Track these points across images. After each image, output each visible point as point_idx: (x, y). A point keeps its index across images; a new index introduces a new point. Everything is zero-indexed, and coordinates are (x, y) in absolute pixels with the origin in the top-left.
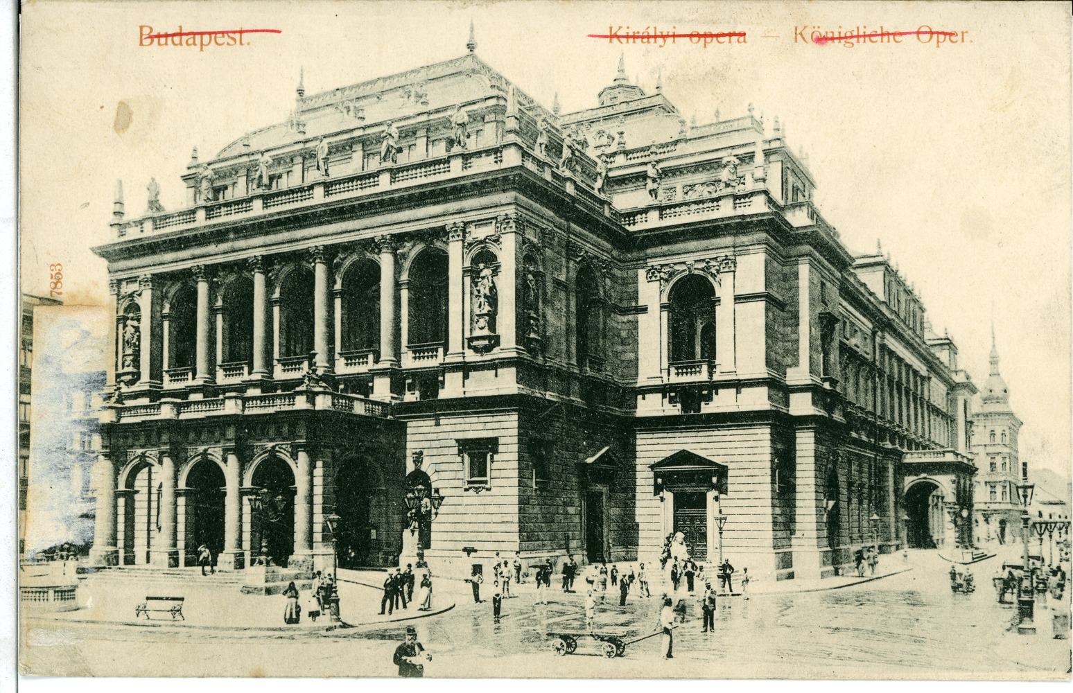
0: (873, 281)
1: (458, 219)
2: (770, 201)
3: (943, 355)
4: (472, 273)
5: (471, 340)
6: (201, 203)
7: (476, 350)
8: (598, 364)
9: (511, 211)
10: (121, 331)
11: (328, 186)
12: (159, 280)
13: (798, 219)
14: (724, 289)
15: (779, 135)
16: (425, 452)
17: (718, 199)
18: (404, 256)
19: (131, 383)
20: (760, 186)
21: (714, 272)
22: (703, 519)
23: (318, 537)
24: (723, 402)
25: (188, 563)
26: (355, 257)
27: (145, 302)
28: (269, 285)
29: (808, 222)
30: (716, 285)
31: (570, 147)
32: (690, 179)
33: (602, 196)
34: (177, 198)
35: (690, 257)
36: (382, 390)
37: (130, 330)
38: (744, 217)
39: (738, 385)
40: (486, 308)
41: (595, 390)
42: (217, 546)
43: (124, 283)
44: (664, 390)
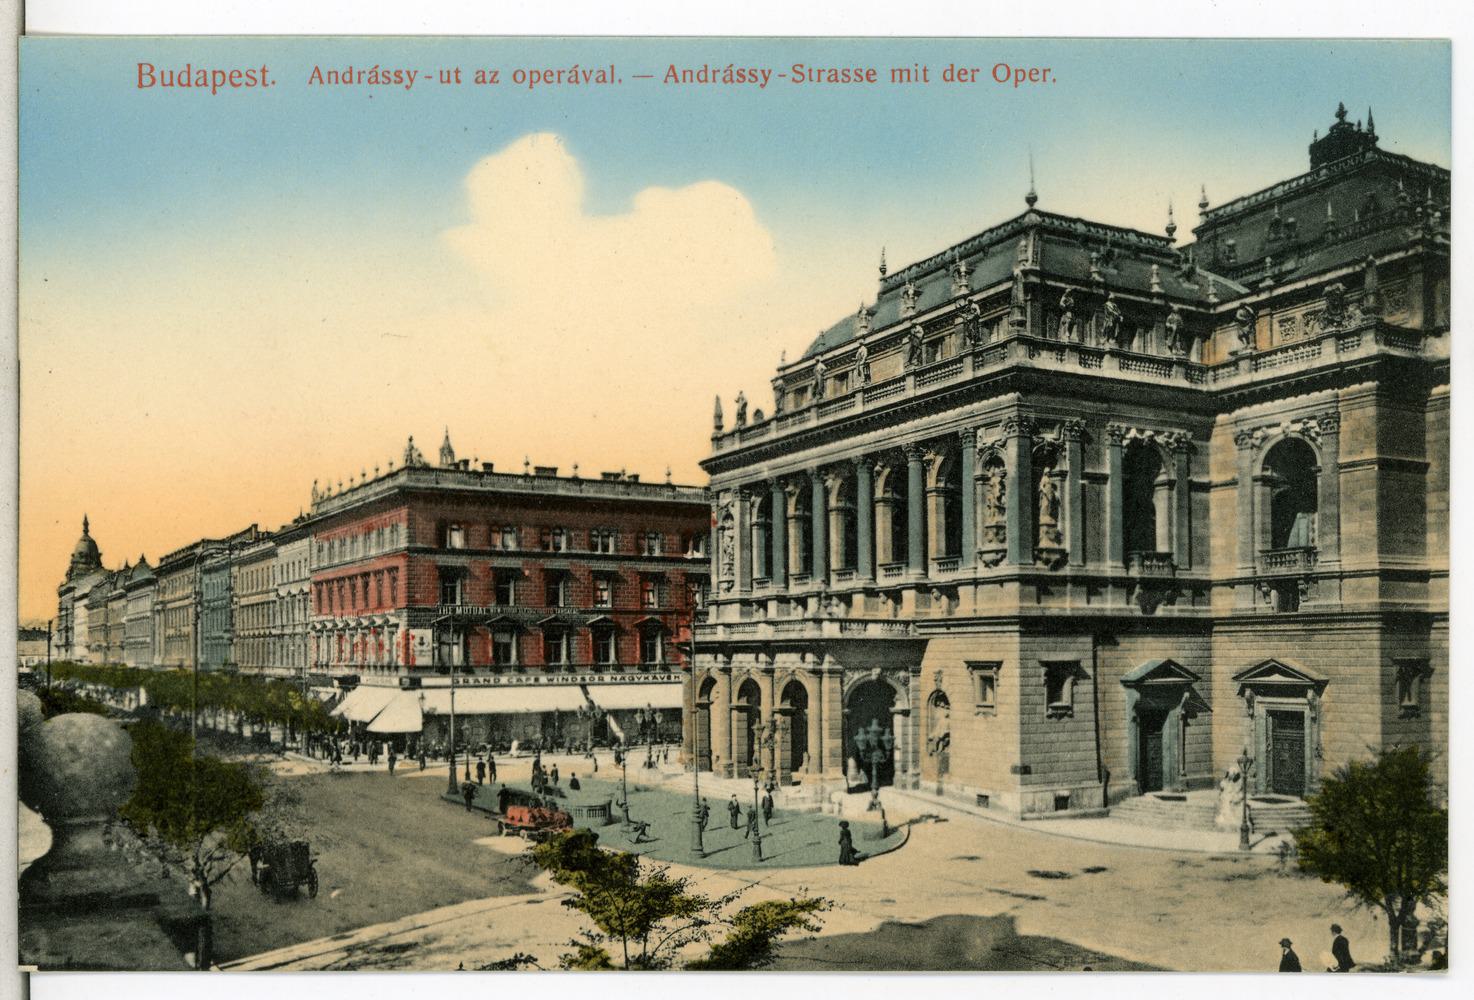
7: (987, 565)
12: (747, 490)
16: (946, 671)
18: (930, 462)
21: (1313, 435)
23: (826, 760)
28: (827, 492)
43: (722, 494)
44: (1254, 582)
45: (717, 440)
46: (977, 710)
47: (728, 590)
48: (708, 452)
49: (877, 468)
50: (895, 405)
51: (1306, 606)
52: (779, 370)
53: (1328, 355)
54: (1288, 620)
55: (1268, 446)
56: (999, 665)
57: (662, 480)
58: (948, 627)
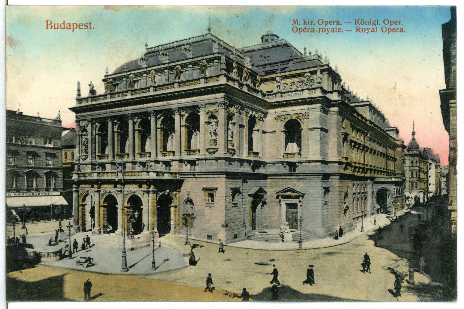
1: (203, 102)
3: (392, 134)
6: (108, 92)
7: (210, 153)
9: (222, 100)
10: (81, 140)
11: (156, 88)
15: (327, 63)
17: (303, 90)
20: (319, 85)
22: (297, 212)
25: (104, 233)
28: (134, 123)
30: (302, 124)
31: (246, 72)
34: (101, 90)
37: (84, 139)
38: (312, 98)
42: (115, 228)
44: (283, 163)
45: (79, 100)
46: (207, 205)
47: (85, 159)
48: (74, 104)
49: (159, 116)
50: (169, 93)
51: (297, 171)
53: (306, 94)
54: (292, 175)
55: (286, 121)
56: (216, 189)
57: (36, 115)
58: (194, 175)
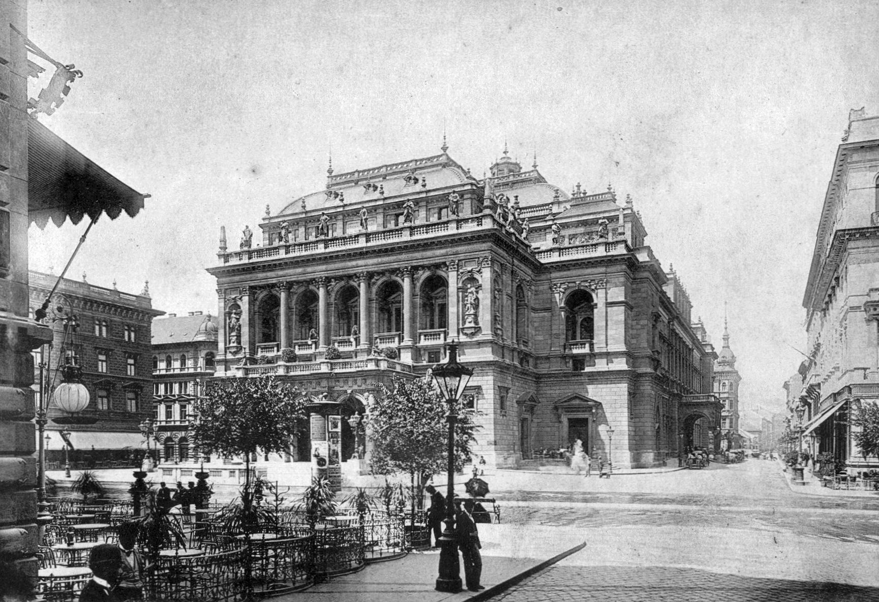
0: (669, 290)
2: (627, 246)
4: (462, 290)
5: (463, 329)
8: (525, 343)
9: (487, 254)
10: (228, 321)
11: (368, 236)
13: (642, 257)
14: (599, 298)
19: (235, 353)
24: (601, 365)
26: (384, 279)
27: (244, 304)
28: (328, 293)
29: (647, 259)
30: (594, 295)
32: (572, 231)
33: (526, 242)
35: (578, 279)
36: (406, 358)
37: (234, 320)
38: (613, 256)
39: (608, 356)
40: (472, 311)
41: (524, 357)
52: (264, 219)
53: (601, 252)
